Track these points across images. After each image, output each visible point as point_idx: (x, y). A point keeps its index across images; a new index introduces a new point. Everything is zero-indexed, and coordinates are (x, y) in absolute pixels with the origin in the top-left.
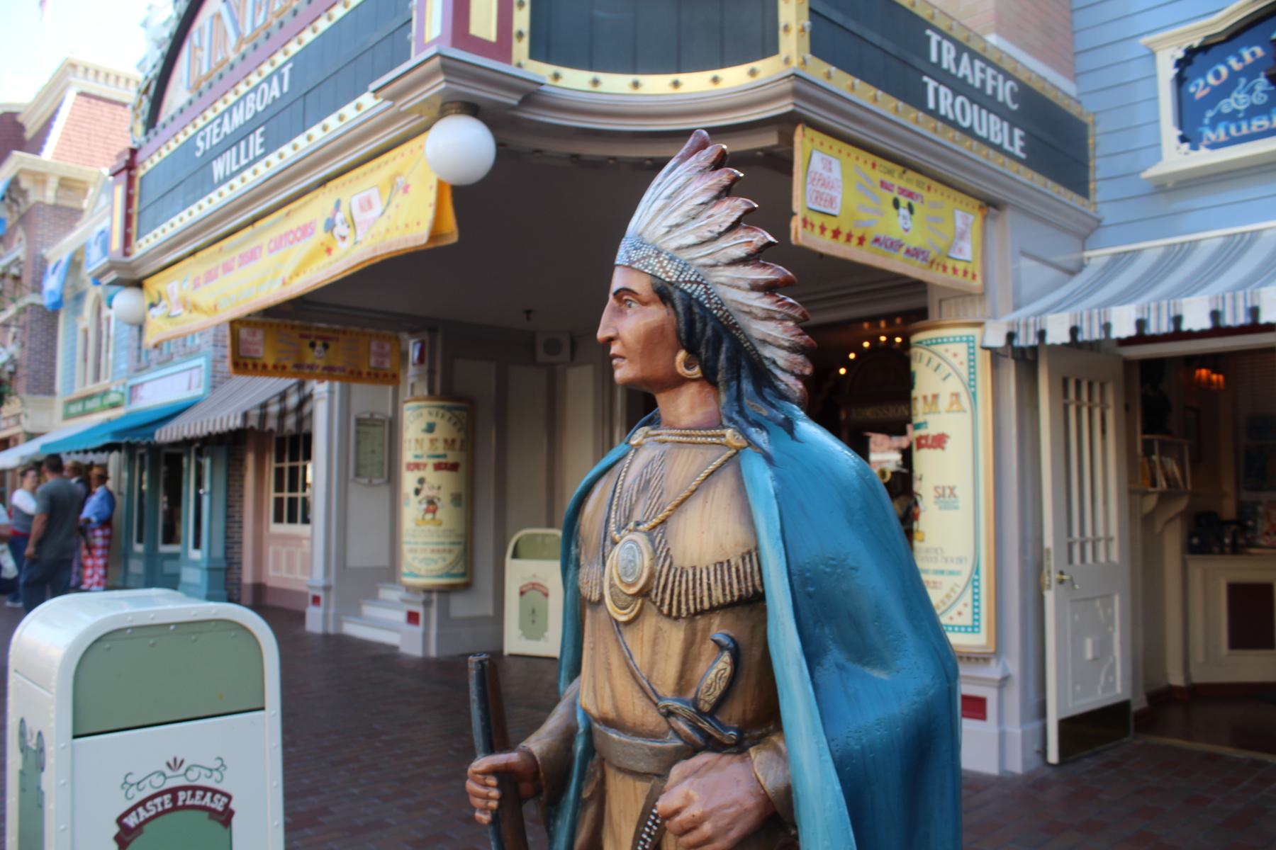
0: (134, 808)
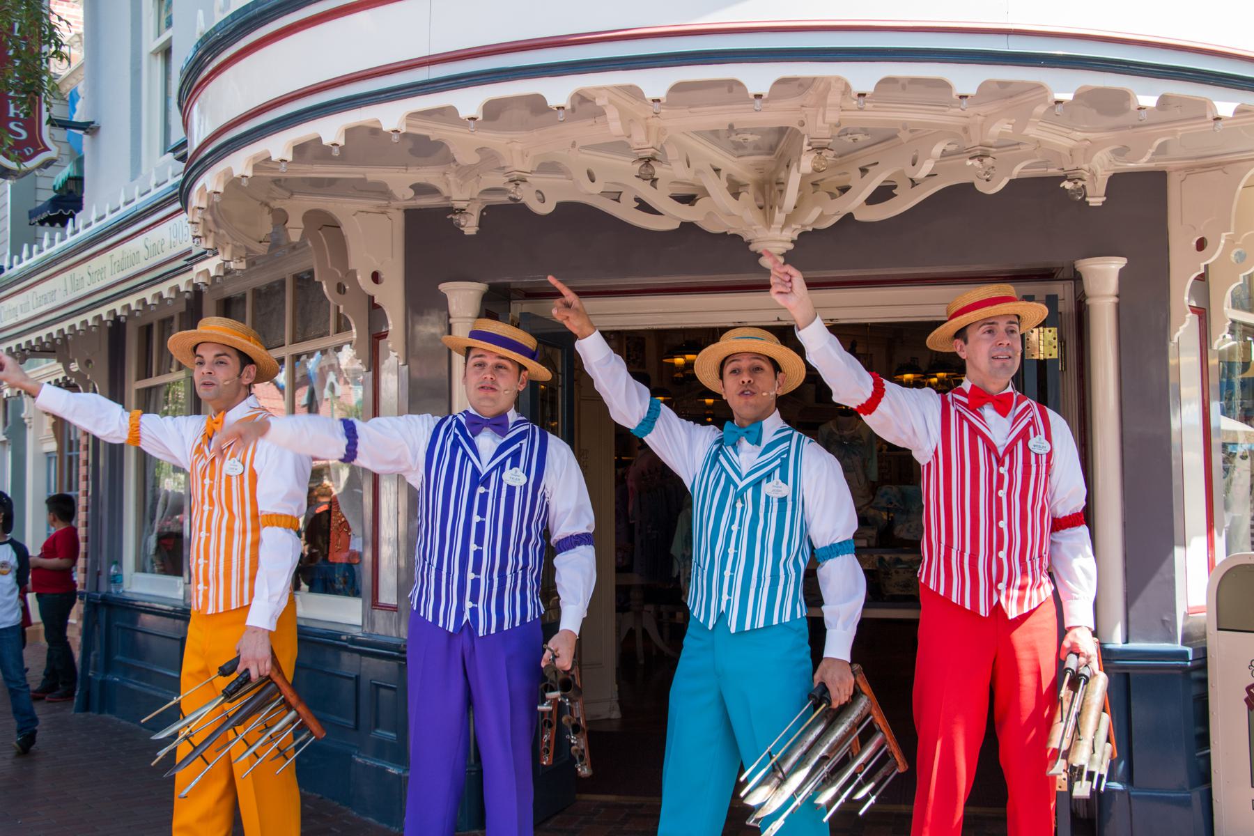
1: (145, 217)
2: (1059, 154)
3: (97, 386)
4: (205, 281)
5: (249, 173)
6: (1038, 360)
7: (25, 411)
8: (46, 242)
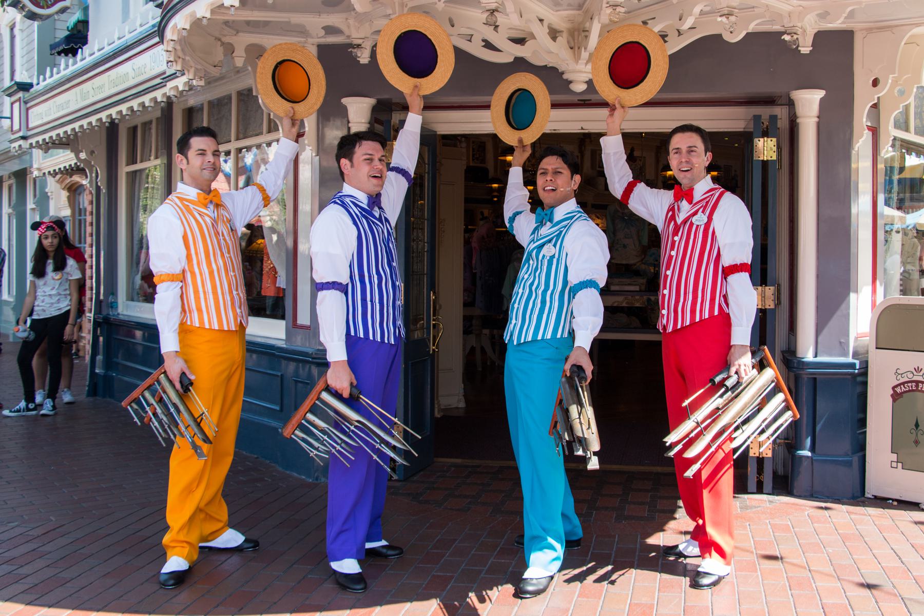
0: (899, 385)
1: (132, 49)
2: (781, 15)
3: (98, 169)
4: (175, 94)
5: (208, 15)
6: (763, 161)
7: (49, 187)
8: (63, 66)
